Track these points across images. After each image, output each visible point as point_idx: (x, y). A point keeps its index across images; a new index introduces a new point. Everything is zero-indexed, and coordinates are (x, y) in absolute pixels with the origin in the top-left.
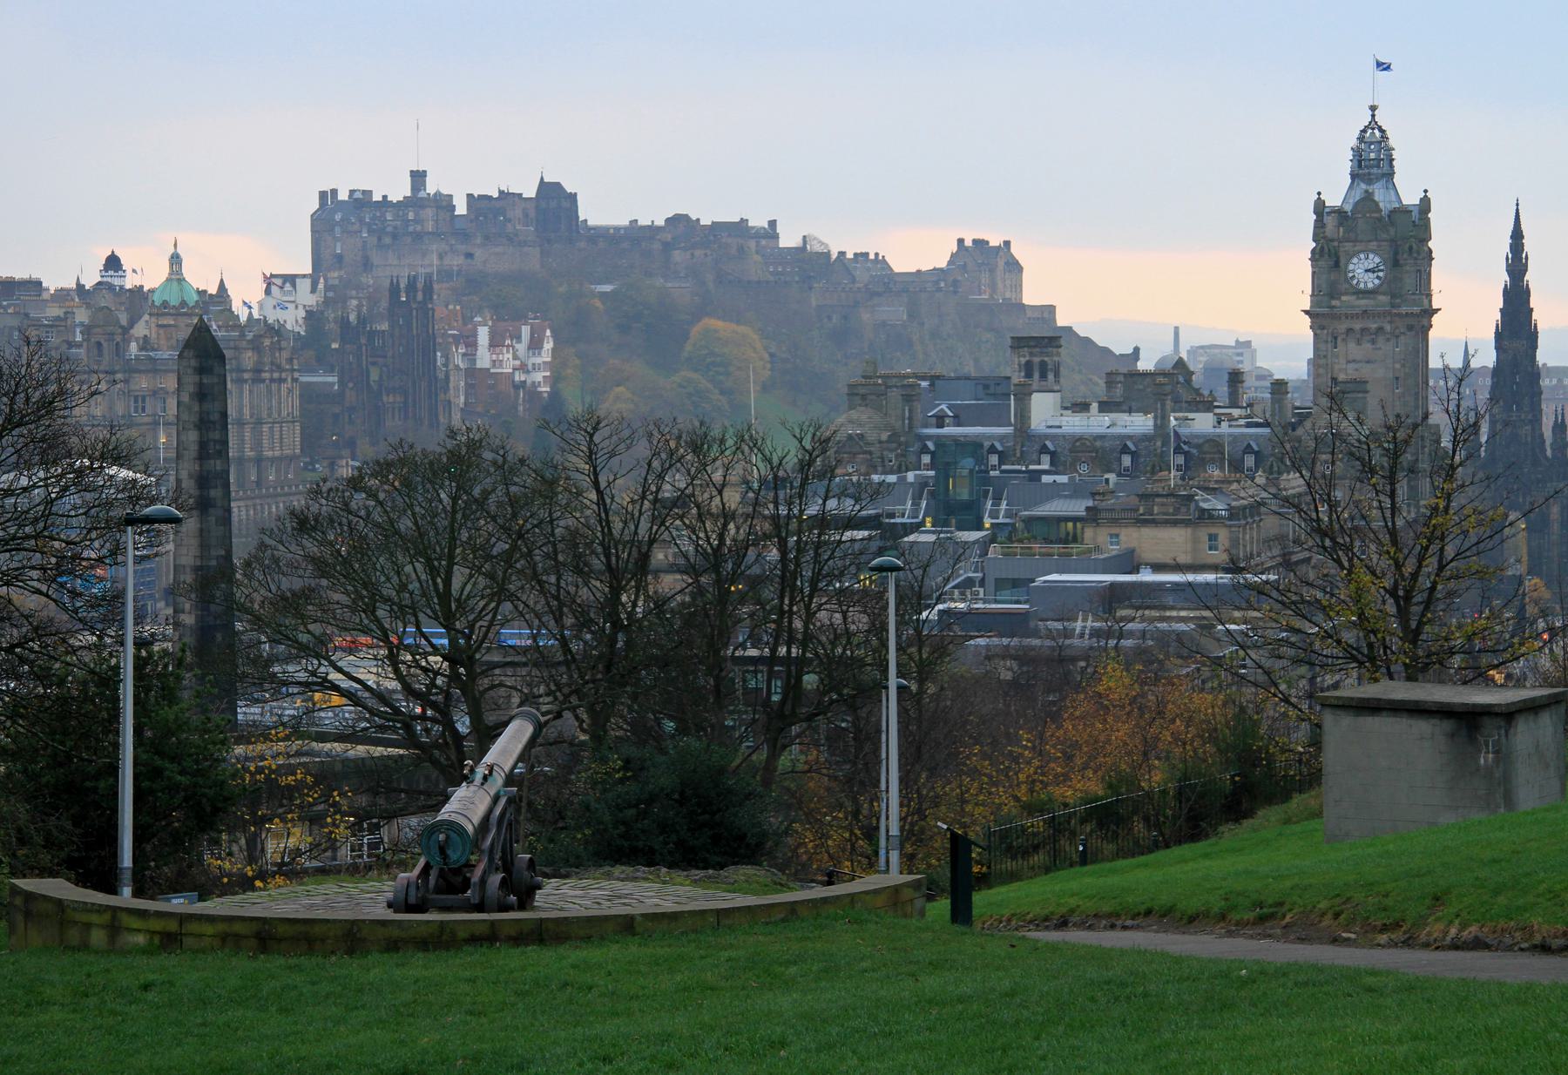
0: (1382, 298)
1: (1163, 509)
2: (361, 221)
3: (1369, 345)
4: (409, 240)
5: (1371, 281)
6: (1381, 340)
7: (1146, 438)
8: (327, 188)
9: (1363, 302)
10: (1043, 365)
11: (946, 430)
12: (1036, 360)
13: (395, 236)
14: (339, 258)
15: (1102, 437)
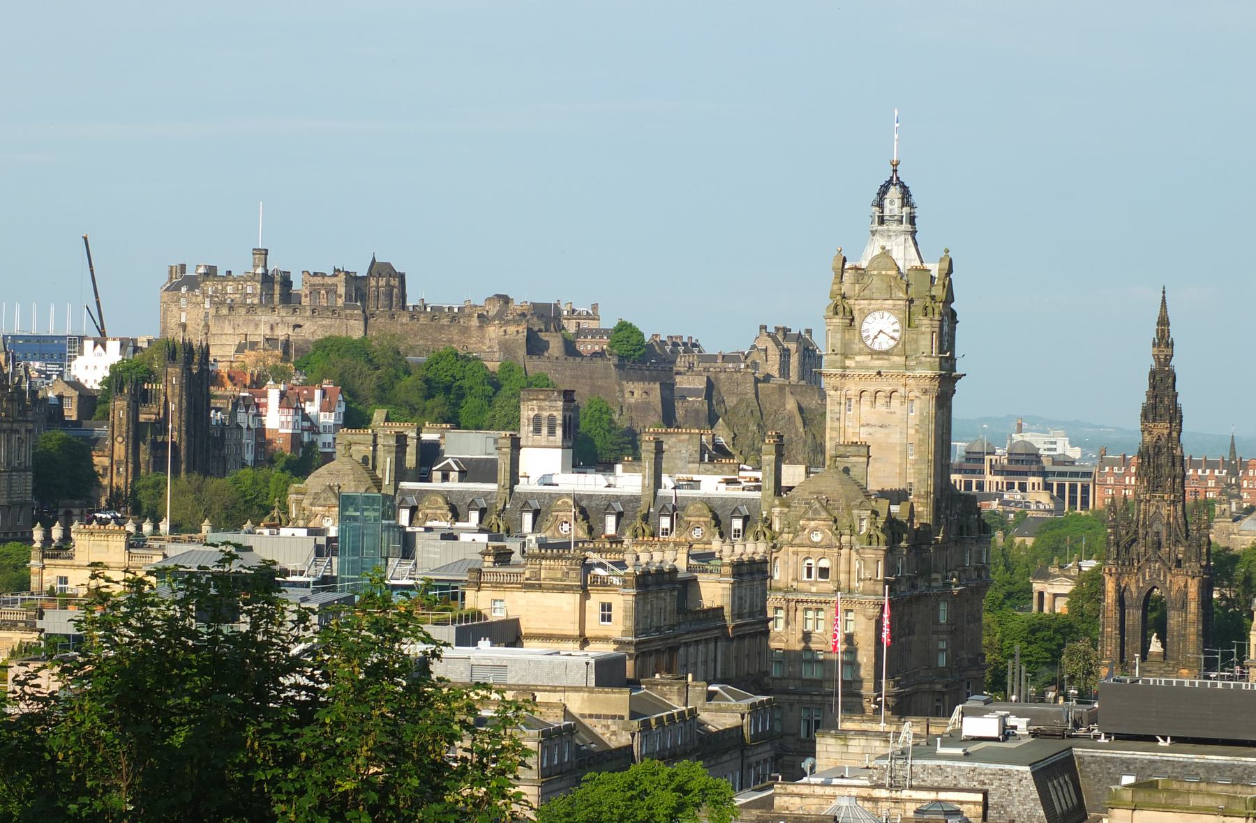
0: (895, 359)
1: (552, 574)
2: (205, 294)
3: (884, 409)
4: (243, 311)
5: (884, 343)
6: (895, 402)
7: (635, 499)
8: (176, 262)
9: (878, 363)
10: (552, 419)
11: (454, 485)
12: (545, 414)
13: (231, 308)
14: (184, 326)
15: (590, 497)
